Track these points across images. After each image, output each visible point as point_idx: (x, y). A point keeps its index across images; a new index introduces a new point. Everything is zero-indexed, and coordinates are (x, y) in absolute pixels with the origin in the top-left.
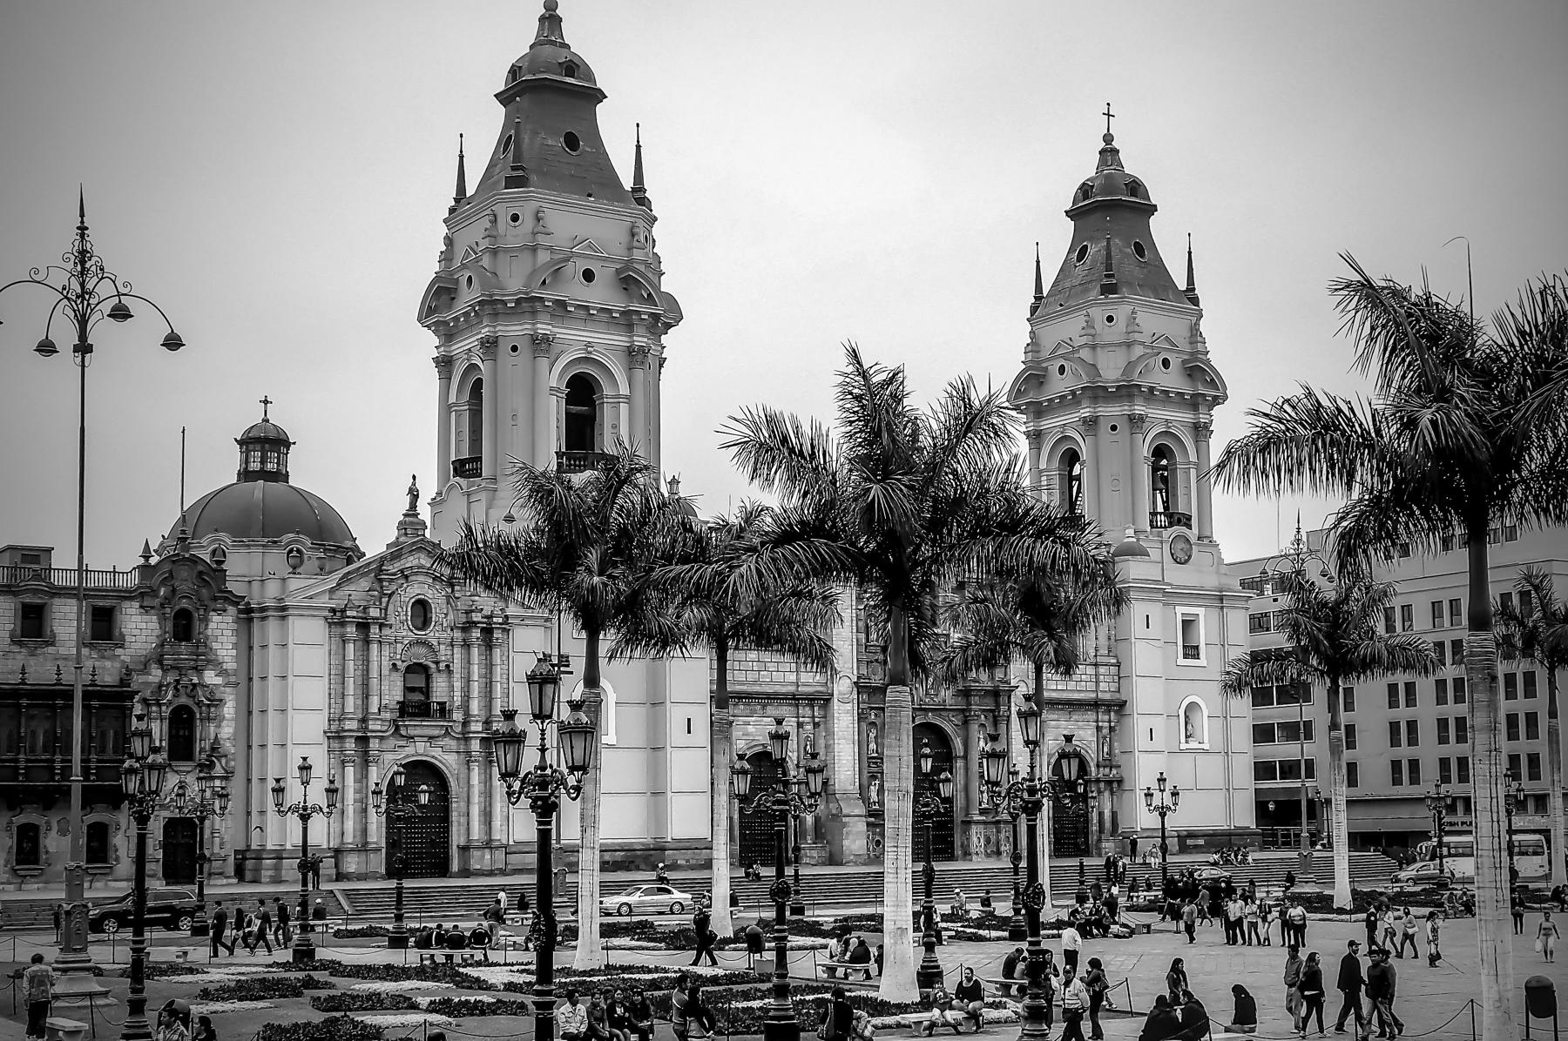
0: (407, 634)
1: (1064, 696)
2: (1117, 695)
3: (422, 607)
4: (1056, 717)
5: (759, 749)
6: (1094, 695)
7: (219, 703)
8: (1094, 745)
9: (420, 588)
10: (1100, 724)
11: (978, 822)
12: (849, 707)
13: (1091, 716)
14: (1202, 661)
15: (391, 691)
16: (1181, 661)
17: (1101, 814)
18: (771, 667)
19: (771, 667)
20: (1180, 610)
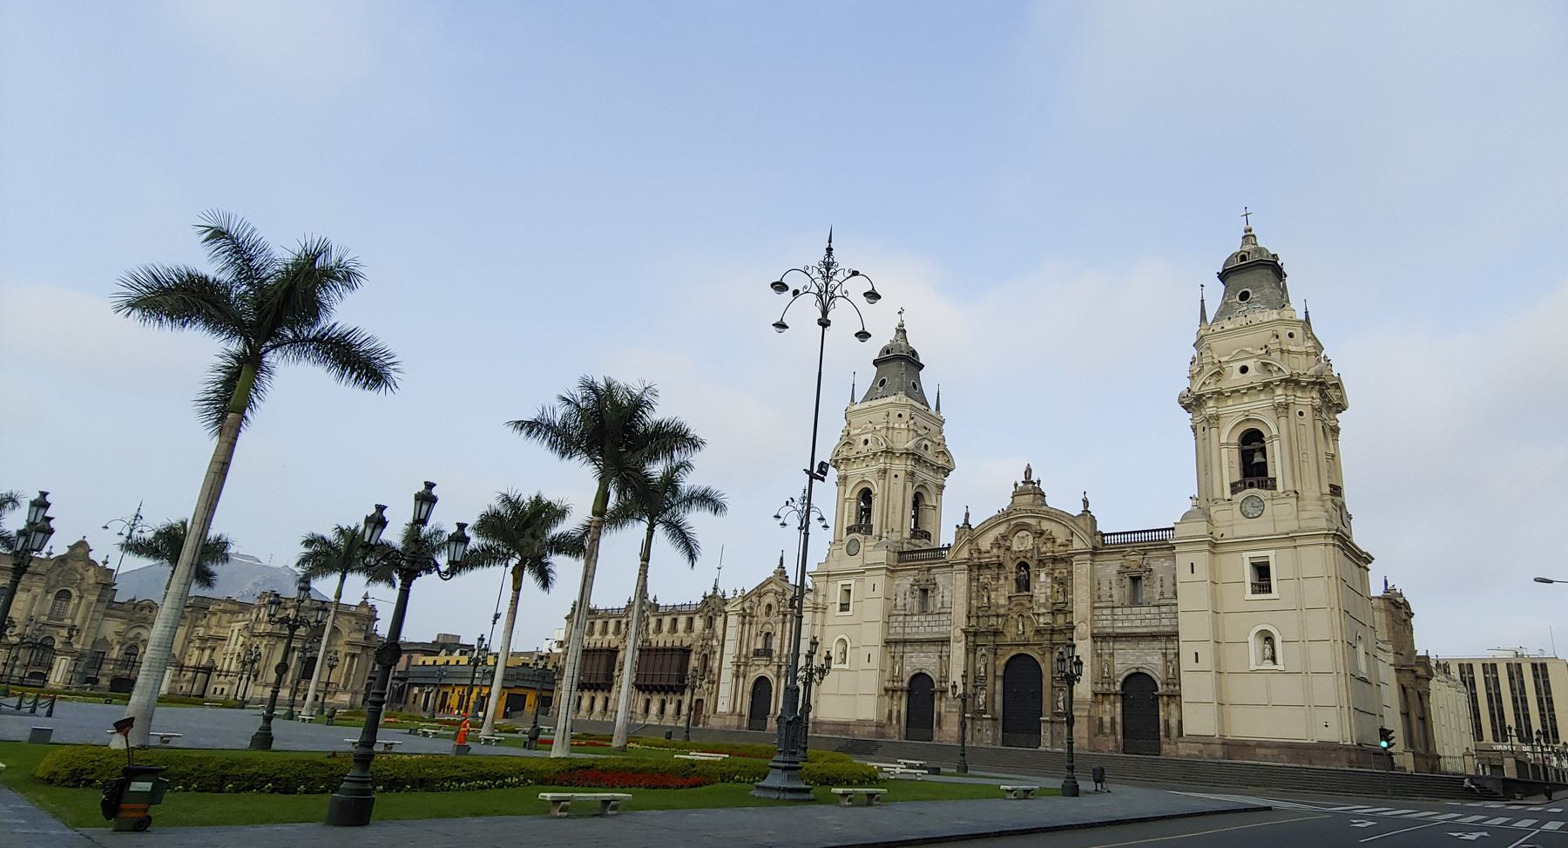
0: (765, 619)
1: (1128, 631)
2: (1176, 630)
3: (769, 606)
4: (1122, 647)
5: (918, 671)
6: (1111, 630)
7: (715, 653)
8: (1161, 668)
9: (770, 599)
10: (1164, 651)
11: (1044, 721)
12: (959, 644)
13: (1156, 644)
14: (1275, 594)
15: (759, 646)
16: (1249, 595)
17: (1167, 722)
18: (926, 624)
19: (926, 624)
20: (1246, 555)
